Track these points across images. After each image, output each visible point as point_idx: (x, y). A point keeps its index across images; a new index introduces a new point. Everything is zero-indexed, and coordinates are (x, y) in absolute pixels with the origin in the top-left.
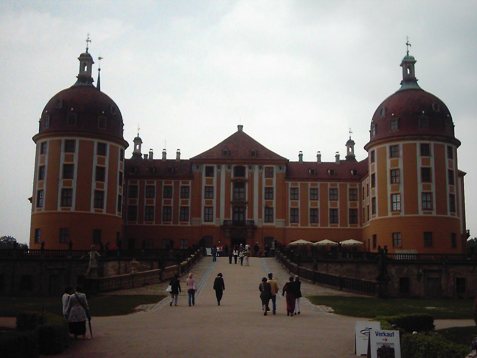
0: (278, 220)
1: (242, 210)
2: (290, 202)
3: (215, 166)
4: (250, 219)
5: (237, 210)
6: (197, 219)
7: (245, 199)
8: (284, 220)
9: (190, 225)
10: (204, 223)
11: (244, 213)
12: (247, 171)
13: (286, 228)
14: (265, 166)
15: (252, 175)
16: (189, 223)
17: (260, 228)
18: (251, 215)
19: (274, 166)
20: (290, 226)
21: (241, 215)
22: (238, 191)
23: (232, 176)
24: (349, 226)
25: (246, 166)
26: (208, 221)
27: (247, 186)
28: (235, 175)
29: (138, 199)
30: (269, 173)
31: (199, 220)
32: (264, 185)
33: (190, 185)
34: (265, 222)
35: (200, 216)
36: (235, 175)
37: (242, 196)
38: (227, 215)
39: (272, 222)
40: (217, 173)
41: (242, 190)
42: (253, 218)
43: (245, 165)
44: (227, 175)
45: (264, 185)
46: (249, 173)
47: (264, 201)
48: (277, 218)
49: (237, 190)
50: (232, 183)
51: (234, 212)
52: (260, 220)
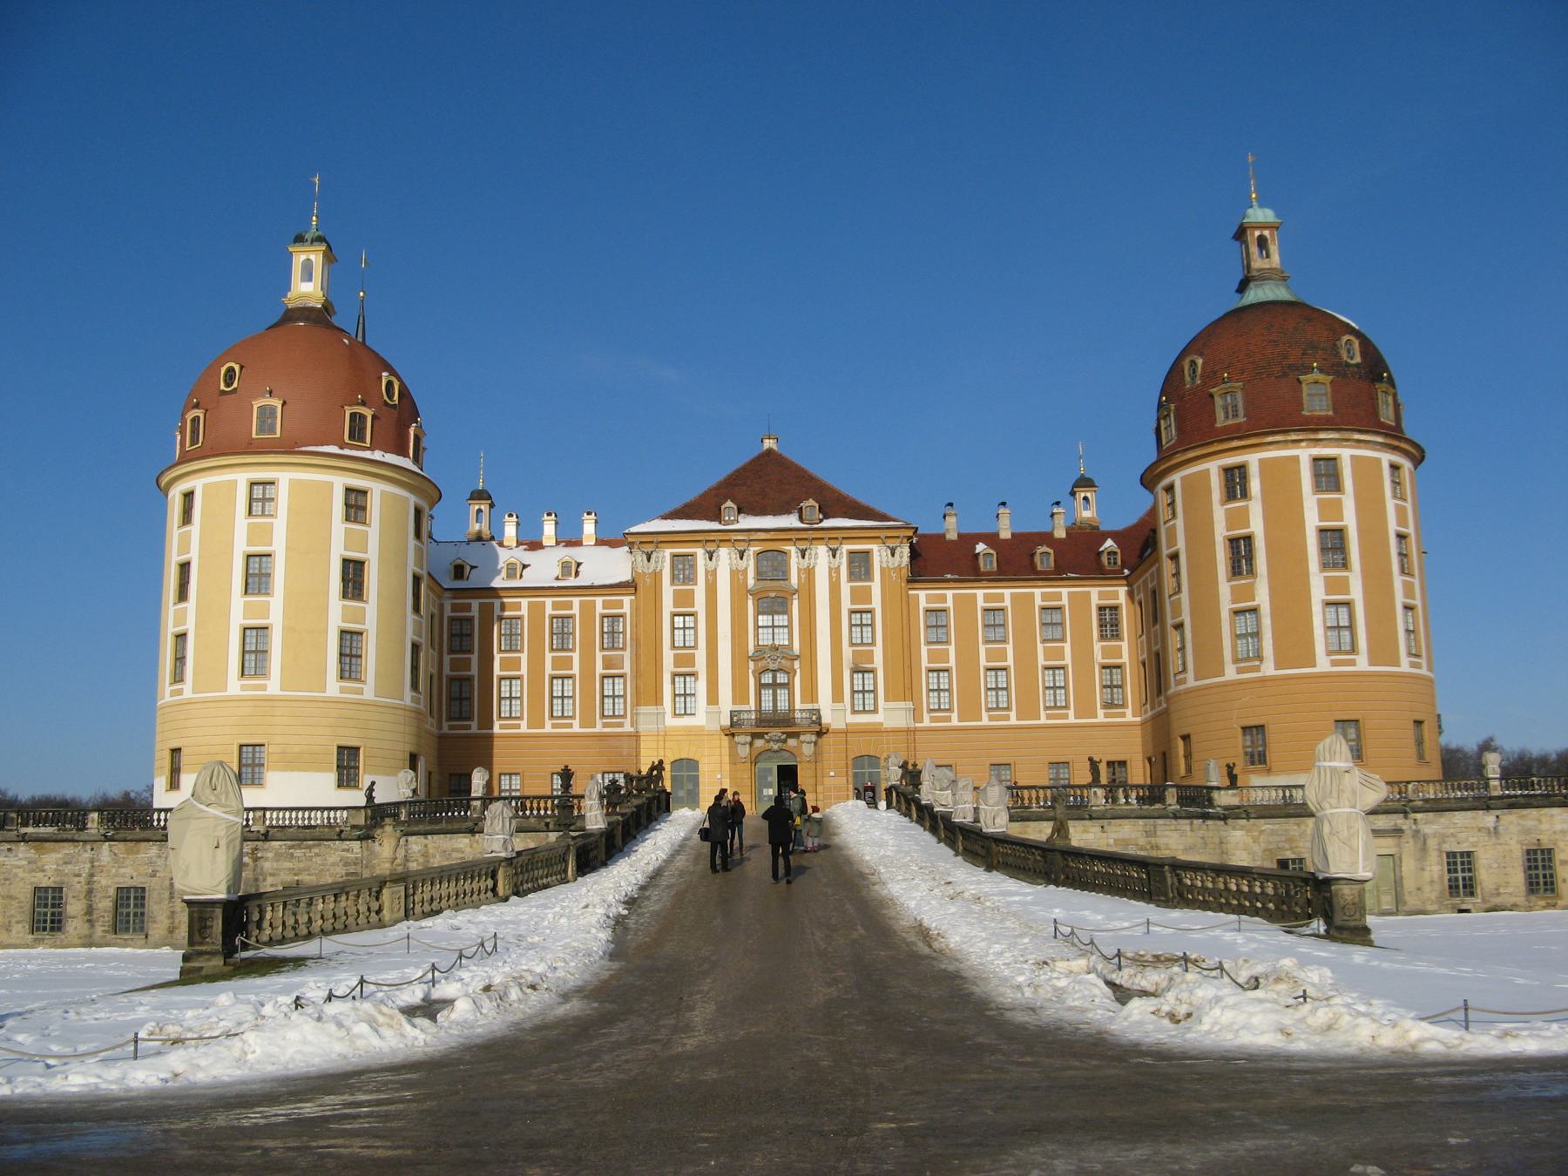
0: (892, 705)
1: (781, 678)
2: (924, 649)
3: (700, 553)
4: (809, 706)
5: (767, 678)
6: (652, 709)
7: (790, 646)
8: (910, 705)
9: (632, 730)
11: (788, 686)
12: (794, 561)
13: (915, 730)
14: (846, 548)
15: (809, 573)
17: (837, 732)
18: (811, 693)
19: (874, 548)
20: (926, 723)
21: (782, 694)
23: (751, 582)
24: (1101, 717)
25: (792, 550)
29: (475, 658)
30: (860, 565)
32: (846, 604)
33: (626, 609)
34: (854, 712)
35: (657, 700)
36: (760, 576)
38: (739, 694)
39: (875, 711)
40: (707, 572)
41: (781, 620)
42: (817, 702)
44: (737, 576)
45: (846, 604)
46: (799, 570)
47: (847, 652)
48: (887, 700)
49: (764, 620)
50: (750, 602)
51: (761, 686)
52: (839, 706)
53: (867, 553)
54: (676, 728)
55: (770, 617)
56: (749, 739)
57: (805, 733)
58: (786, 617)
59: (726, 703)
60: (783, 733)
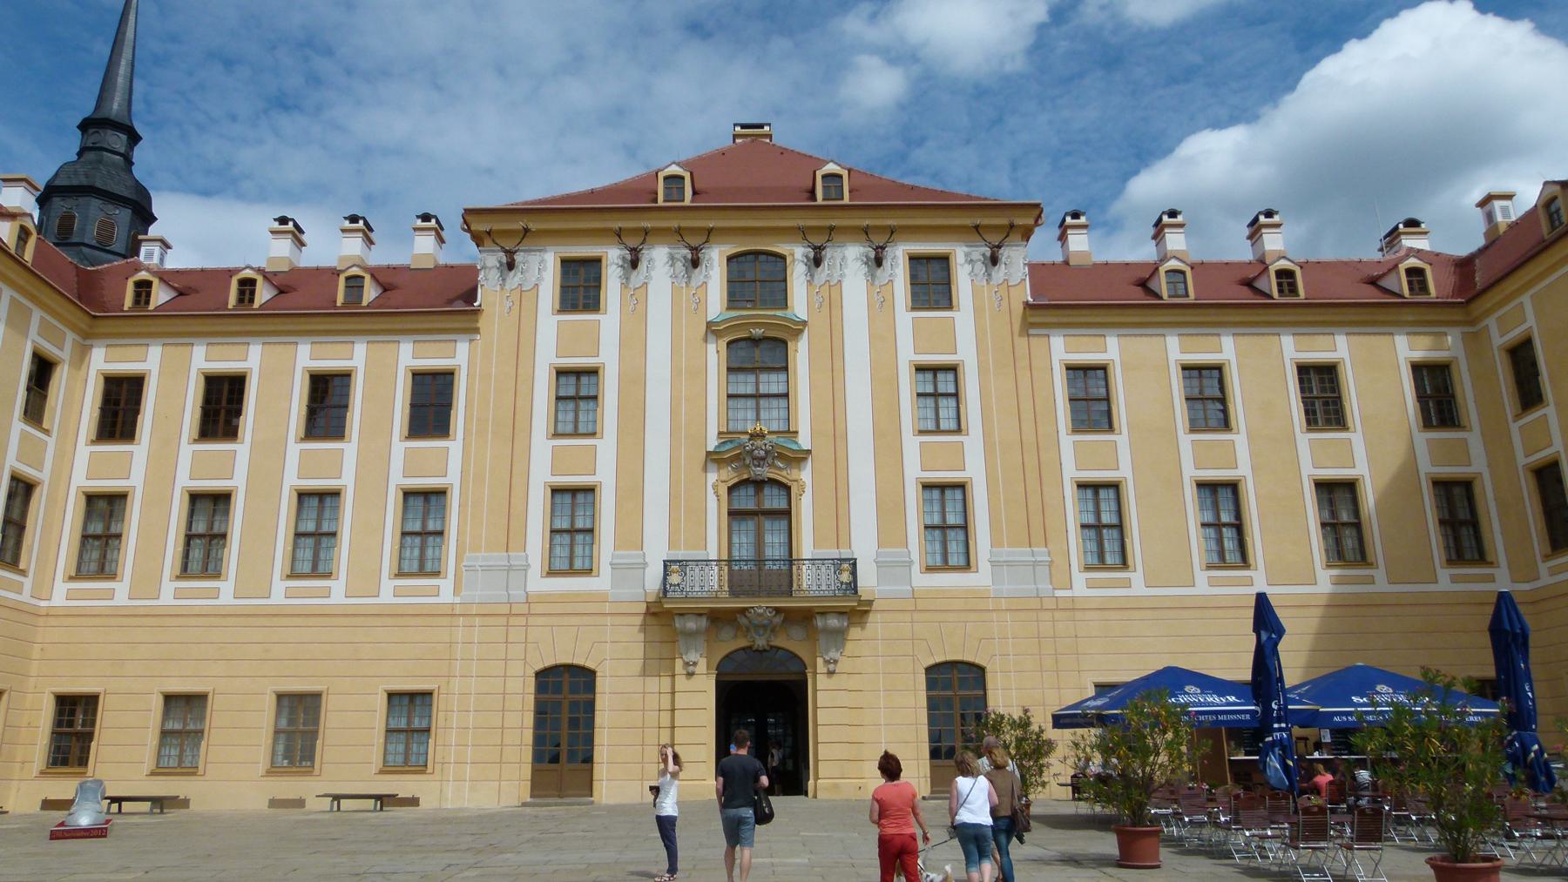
0: (1006, 553)
1: (773, 500)
5: (746, 501)
10: (538, 583)
16: (446, 585)
22: (750, 390)
25: (797, 253)
26: (571, 572)
27: (801, 353)
28: (733, 301)
31: (510, 568)
37: (771, 419)
41: (770, 383)
43: (781, 248)
49: (745, 384)
50: (712, 348)
53: (944, 260)
54: (546, 599)
55: (751, 378)
56: (703, 622)
57: (824, 613)
58: (782, 377)
59: (657, 550)
60: (778, 610)
